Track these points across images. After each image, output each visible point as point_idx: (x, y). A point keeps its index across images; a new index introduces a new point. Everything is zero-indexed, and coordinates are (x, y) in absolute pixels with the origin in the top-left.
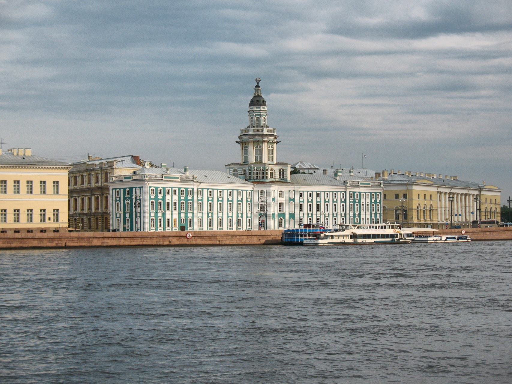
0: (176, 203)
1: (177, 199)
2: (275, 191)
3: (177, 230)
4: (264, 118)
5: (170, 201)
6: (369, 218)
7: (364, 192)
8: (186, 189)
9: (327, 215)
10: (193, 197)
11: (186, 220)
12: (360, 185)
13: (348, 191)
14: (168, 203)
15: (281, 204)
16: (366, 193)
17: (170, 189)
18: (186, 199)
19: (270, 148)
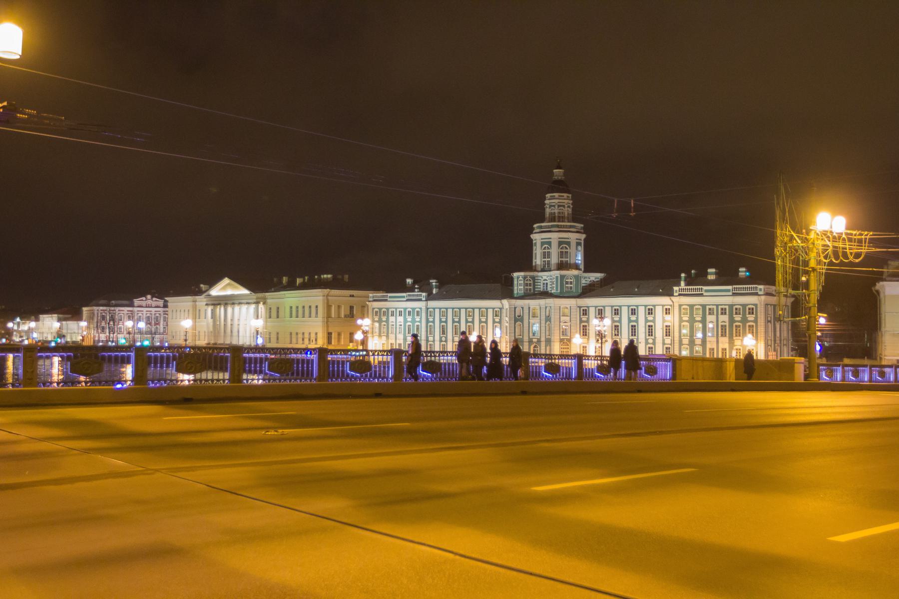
2: (523, 308)
4: (562, 210)
5: (394, 324)
6: (727, 346)
7: (713, 305)
8: (413, 309)
10: (421, 318)
16: (720, 307)
17: (394, 310)
18: (414, 321)
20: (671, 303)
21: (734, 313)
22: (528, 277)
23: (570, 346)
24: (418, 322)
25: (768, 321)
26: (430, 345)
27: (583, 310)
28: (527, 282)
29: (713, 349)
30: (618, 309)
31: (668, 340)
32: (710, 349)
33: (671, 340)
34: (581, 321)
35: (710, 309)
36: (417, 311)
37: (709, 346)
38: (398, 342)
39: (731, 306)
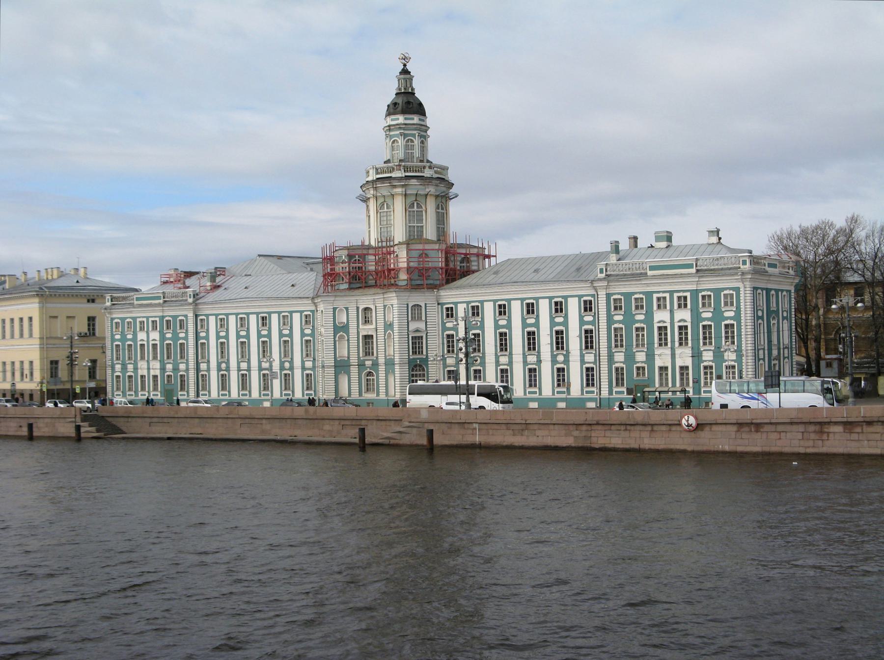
0: (155, 346)
1: (158, 338)
2: (347, 309)
3: (159, 397)
5: (145, 343)
6: (688, 362)
9: (532, 359)
10: (187, 332)
11: (176, 378)
12: (650, 273)
13: (602, 294)
14: (142, 346)
15: (368, 338)
16: (676, 295)
17: (145, 320)
18: (175, 337)
19: (386, 210)
20: (595, 293)
21: (700, 306)
22: (357, 256)
23: (428, 372)
24: (182, 338)
25: (759, 318)
26: (202, 375)
27: (447, 309)
28: (354, 265)
29: (666, 368)
30: (505, 305)
31: (590, 358)
32: (661, 368)
33: (595, 356)
34: (445, 328)
35: (659, 299)
36: (180, 321)
37: (658, 363)
38: (152, 373)
39: (695, 293)
